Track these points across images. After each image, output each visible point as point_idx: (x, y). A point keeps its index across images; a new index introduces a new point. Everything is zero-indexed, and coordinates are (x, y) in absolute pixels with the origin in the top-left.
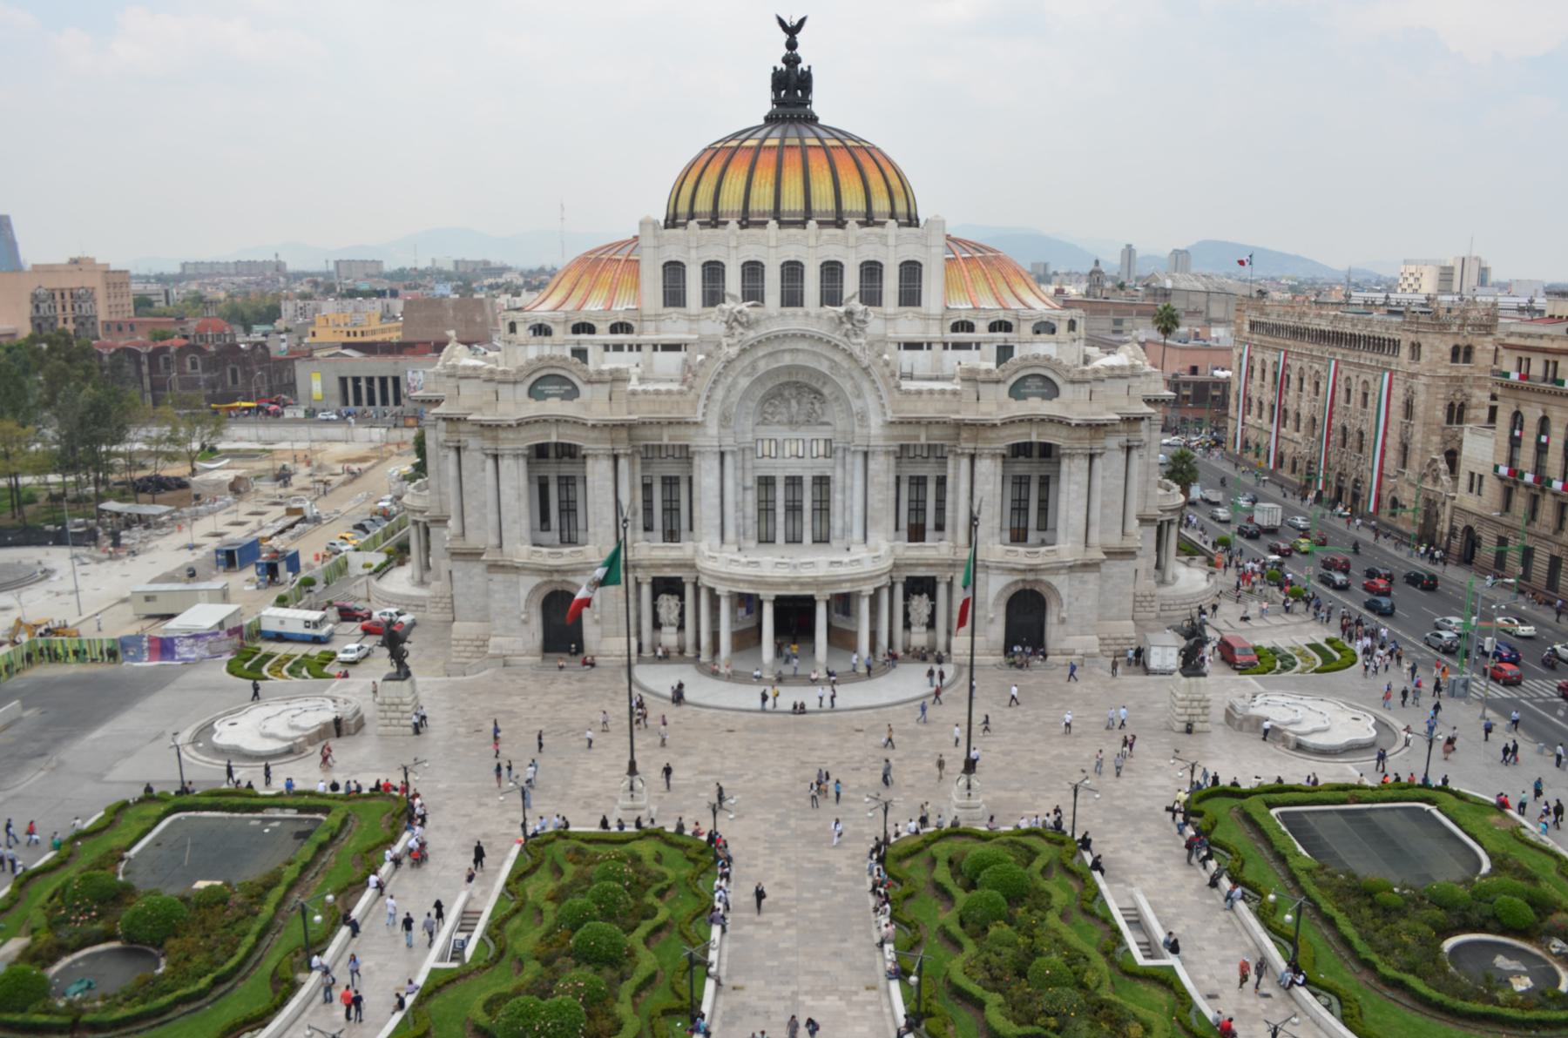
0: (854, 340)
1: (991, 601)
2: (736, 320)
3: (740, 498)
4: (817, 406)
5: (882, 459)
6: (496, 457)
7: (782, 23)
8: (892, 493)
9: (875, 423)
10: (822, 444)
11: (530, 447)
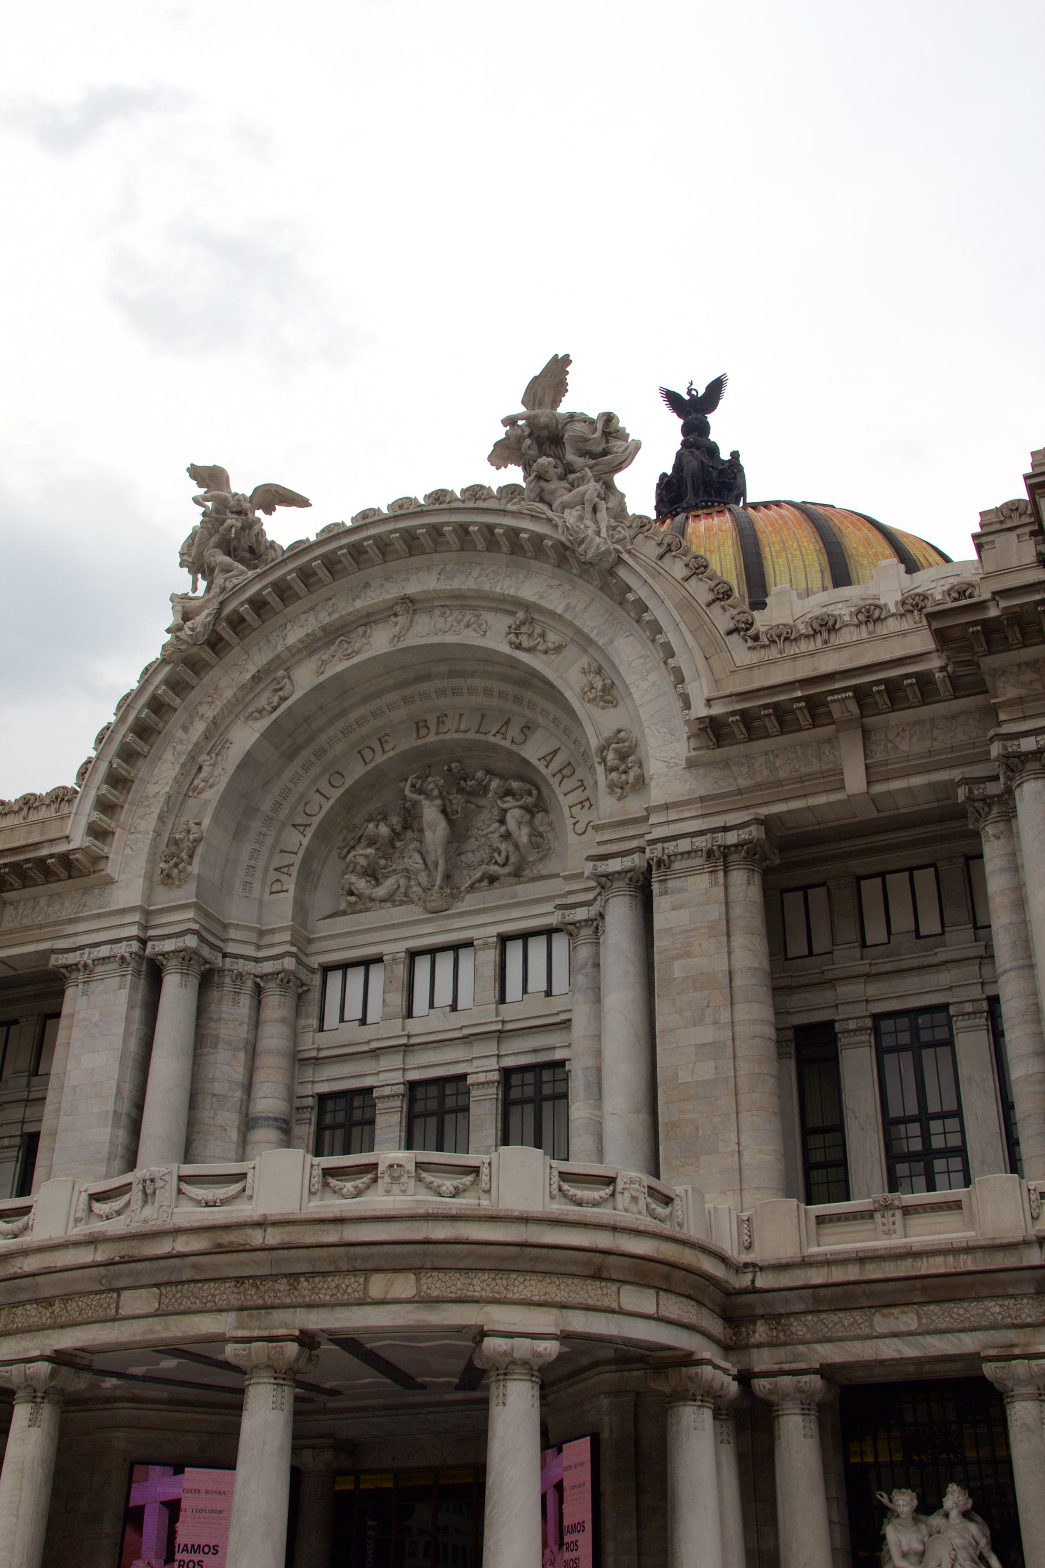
7: (673, 399)
9: (667, 757)
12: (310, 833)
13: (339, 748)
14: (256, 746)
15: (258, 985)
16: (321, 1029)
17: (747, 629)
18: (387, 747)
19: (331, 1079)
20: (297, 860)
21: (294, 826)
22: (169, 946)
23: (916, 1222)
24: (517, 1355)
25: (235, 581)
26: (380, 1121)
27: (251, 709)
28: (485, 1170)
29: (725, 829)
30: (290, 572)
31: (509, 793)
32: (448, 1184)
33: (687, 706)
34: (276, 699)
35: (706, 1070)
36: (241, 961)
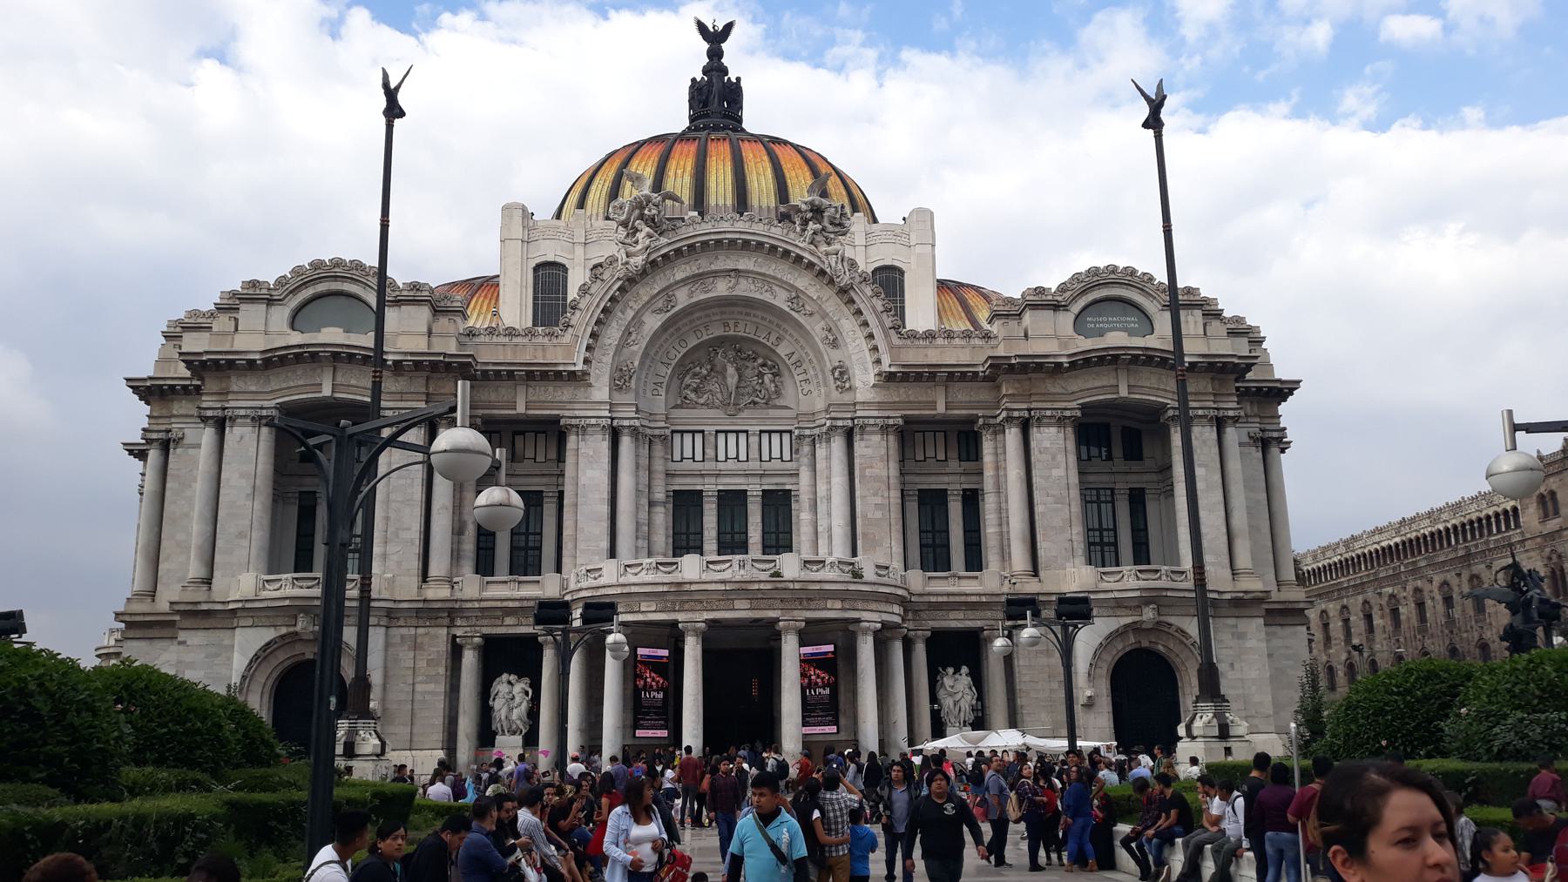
0: (824, 248)
2: (641, 217)
3: (644, 516)
4: (767, 379)
5: (877, 438)
6: (220, 425)
7: (701, 27)
8: (895, 495)
9: (864, 379)
10: (775, 438)
11: (281, 408)
19: (681, 484)
22: (626, 423)
23: (964, 582)
26: (706, 507)
27: (654, 307)
31: (764, 365)
33: (878, 362)
35: (878, 515)
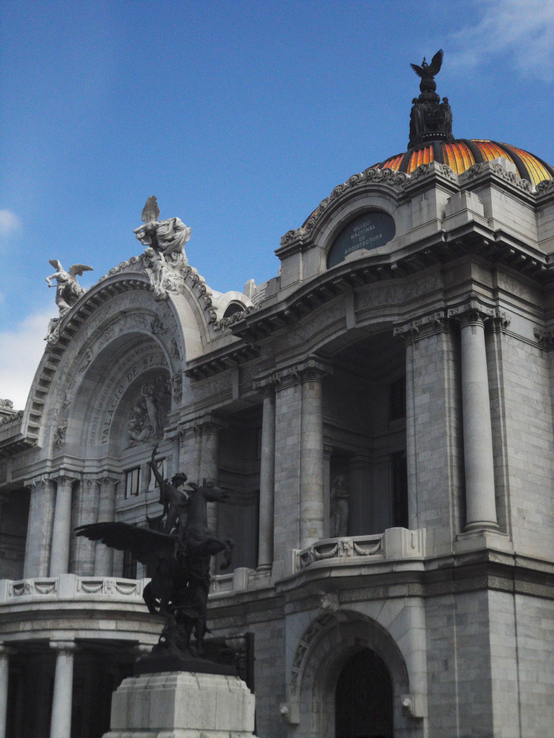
1: (289, 677)
12: (114, 414)
13: (120, 375)
14: (83, 382)
15: (98, 483)
16: (126, 498)
17: (215, 321)
18: (136, 373)
20: (109, 427)
21: (109, 412)
24: (60, 647)
25: (64, 313)
27: (81, 367)
28: (56, 584)
29: (200, 417)
30: (81, 307)
32: (44, 589)
34: (87, 362)
36: (89, 475)
